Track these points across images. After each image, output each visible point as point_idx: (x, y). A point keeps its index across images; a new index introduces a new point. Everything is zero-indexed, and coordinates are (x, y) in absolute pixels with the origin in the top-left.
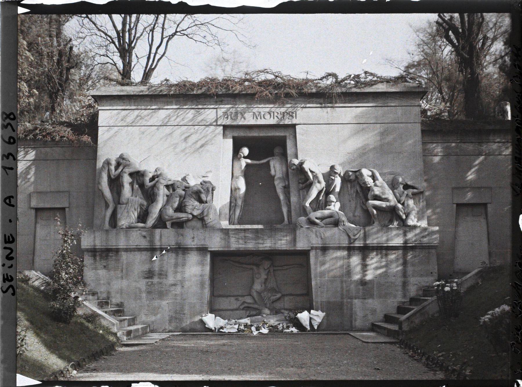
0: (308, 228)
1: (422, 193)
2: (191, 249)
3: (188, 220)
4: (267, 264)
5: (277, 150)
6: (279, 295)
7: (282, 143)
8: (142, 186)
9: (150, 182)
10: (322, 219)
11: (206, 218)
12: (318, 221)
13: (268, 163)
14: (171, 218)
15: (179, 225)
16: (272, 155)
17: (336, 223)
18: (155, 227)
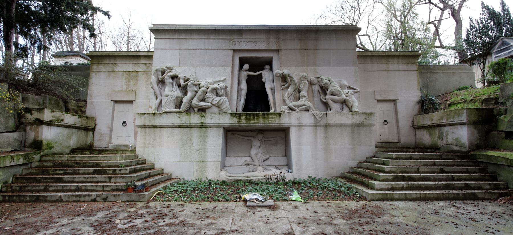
1: (359, 92)
2: (210, 127)
3: (209, 108)
4: (260, 136)
5: (267, 67)
6: (267, 156)
7: (269, 63)
8: (179, 86)
10: (298, 107)
11: (221, 106)
12: (295, 108)
13: (261, 74)
15: (202, 110)
16: (264, 69)
17: (307, 110)
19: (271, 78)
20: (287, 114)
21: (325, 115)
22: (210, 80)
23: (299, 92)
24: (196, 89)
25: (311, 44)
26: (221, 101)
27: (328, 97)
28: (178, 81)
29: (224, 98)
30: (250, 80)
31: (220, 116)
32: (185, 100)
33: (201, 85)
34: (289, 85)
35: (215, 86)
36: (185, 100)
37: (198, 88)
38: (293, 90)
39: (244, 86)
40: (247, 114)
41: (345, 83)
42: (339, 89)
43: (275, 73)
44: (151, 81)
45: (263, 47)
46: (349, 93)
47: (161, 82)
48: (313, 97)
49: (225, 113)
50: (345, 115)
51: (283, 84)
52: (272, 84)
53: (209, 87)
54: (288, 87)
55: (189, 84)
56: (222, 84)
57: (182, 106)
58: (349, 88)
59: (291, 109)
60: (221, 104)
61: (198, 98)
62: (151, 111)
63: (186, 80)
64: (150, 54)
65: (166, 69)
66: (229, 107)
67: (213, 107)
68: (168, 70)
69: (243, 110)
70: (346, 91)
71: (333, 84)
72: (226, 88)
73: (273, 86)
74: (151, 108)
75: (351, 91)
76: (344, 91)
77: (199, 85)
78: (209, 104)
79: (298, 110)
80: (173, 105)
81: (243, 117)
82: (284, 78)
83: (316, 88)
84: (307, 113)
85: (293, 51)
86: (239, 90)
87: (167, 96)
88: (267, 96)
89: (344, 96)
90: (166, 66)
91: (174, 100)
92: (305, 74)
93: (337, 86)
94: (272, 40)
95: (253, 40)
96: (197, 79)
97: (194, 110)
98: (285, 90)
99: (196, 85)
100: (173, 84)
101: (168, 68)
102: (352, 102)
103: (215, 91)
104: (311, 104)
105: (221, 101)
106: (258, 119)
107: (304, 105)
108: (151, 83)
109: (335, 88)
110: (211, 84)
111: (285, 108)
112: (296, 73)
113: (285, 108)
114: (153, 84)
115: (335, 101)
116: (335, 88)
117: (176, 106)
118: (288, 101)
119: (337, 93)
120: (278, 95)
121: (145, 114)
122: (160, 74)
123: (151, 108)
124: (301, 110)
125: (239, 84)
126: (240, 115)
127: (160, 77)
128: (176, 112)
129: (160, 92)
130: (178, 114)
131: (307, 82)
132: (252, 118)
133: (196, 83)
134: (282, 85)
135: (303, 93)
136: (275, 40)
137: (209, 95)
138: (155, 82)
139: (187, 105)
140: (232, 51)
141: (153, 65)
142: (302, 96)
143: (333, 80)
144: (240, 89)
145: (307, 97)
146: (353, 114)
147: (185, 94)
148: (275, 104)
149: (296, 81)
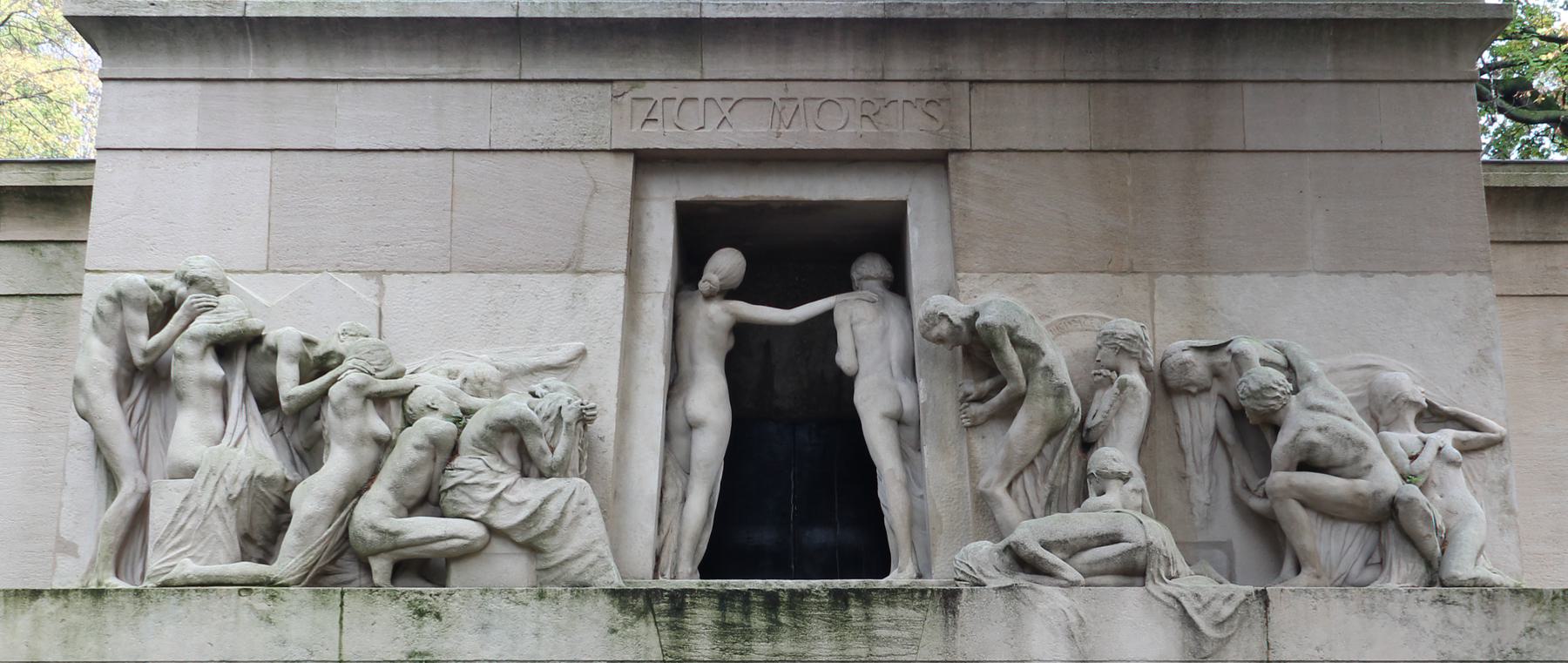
0: (1009, 588)
3: (468, 553)
5: (870, 268)
7: (884, 235)
8: (267, 401)
9: (301, 383)
10: (1072, 548)
11: (550, 543)
12: (1053, 558)
13: (829, 314)
14: (390, 543)
15: (424, 568)
16: (846, 286)
17: (1133, 571)
18: (319, 576)
19: (896, 343)
20: (999, 600)
21: (1256, 607)
22: (480, 364)
23: (1087, 446)
24: (379, 426)
25: (1167, 117)
26: (553, 509)
27: (1280, 478)
28: (260, 369)
29: (574, 485)
30: (747, 355)
31: (544, 614)
32: (311, 498)
33: (414, 401)
34: (1017, 401)
35: (514, 404)
36: (311, 498)
37: (398, 421)
38: (1038, 431)
39: (710, 401)
40: (725, 600)
41: (1409, 382)
42: (1361, 430)
43: (919, 313)
44: (81, 369)
45: (844, 139)
46: (1429, 454)
47: (147, 378)
48: (1184, 477)
49: (579, 588)
50: (1395, 608)
51: (971, 388)
52: (904, 387)
53: (467, 412)
54: (1007, 413)
55: (335, 392)
56: (560, 395)
57: (290, 538)
58: (1432, 416)
59: (1024, 563)
60: (552, 531)
61: (396, 488)
62: (69, 574)
63: (317, 365)
64: (64, 178)
65: (181, 289)
66: (604, 548)
67: (498, 546)
68: (192, 298)
69: (708, 568)
70: (1407, 436)
71: (1311, 394)
72: (585, 419)
73: (908, 405)
74: (69, 548)
75: (1446, 437)
76: (1393, 436)
77: (402, 396)
78: (475, 531)
79: (1071, 573)
80: (225, 531)
81: (702, 617)
82: (977, 350)
83: (1201, 419)
84: (1133, 593)
85: (1045, 160)
86: (677, 431)
87: (190, 472)
88: (867, 471)
89: (1385, 479)
90: (180, 266)
91: (233, 501)
92: (1127, 326)
93: (1344, 405)
94: (901, 92)
95: (775, 91)
96: (389, 360)
97: (367, 568)
98: (993, 430)
99: (380, 400)
100: (223, 389)
101: (192, 282)
102: (1449, 512)
103: (509, 439)
104: (1158, 534)
105: (553, 509)
106: (798, 631)
107: (1113, 539)
108: (78, 384)
109: (1322, 419)
110: (479, 386)
111: (982, 552)
112: (1057, 317)
113: (982, 552)
114: (93, 389)
115: (1327, 510)
116: (1322, 419)
117: (246, 538)
118: (1008, 508)
119: (1340, 453)
120: (938, 466)
121: (36, 594)
122: (143, 320)
123: (69, 548)
124: (1090, 572)
125: (676, 384)
126: (678, 602)
127: (142, 342)
128: (247, 585)
129: (137, 441)
130: (258, 599)
131: (1135, 377)
132: (758, 621)
133: (383, 385)
134: (966, 399)
135: (1116, 454)
136: (922, 90)
137: (469, 464)
138: (106, 377)
139: (323, 532)
140: (629, 163)
141: (93, 254)
142: (1105, 476)
143: (1314, 366)
144: (679, 422)
145: (1138, 481)
146: (1442, 600)
147: (309, 455)
148: (917, 521)
149: (1063, 375)
